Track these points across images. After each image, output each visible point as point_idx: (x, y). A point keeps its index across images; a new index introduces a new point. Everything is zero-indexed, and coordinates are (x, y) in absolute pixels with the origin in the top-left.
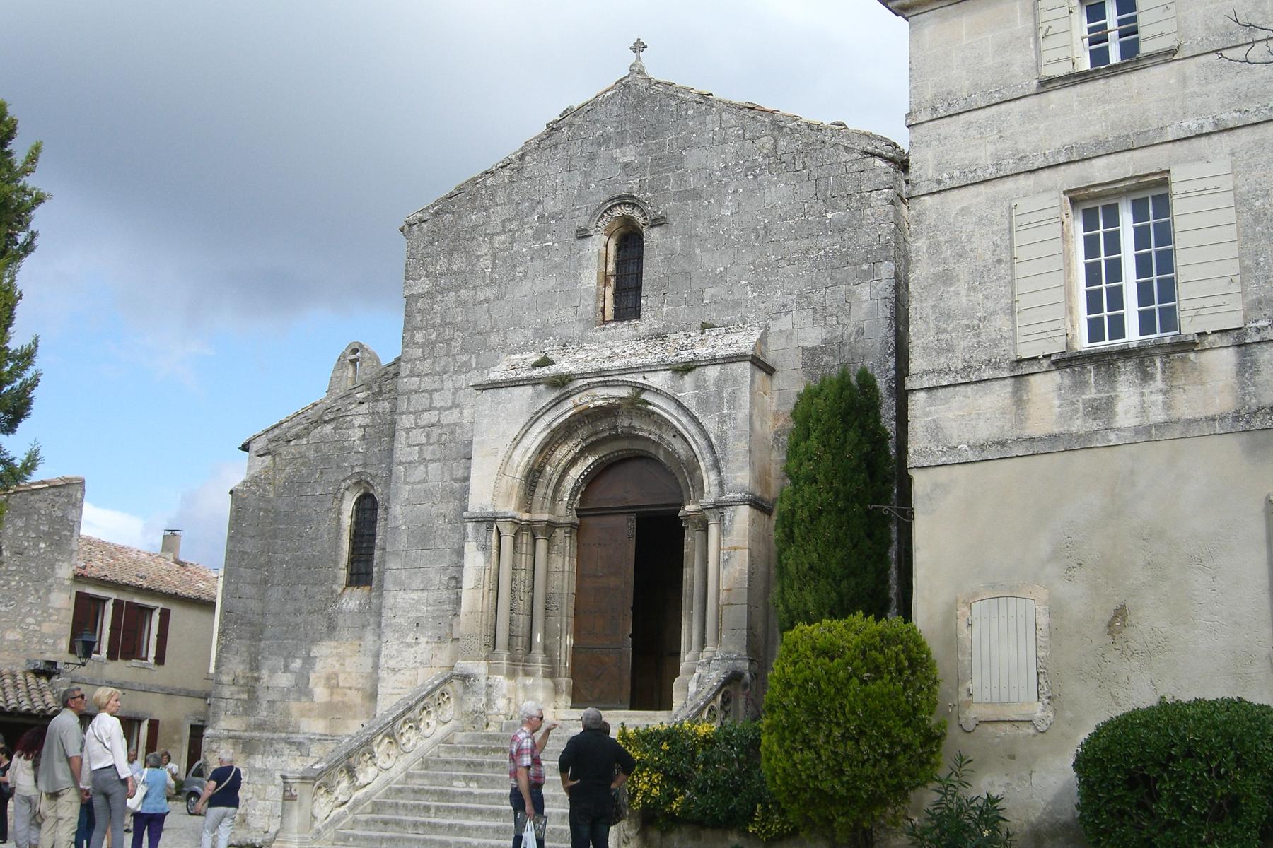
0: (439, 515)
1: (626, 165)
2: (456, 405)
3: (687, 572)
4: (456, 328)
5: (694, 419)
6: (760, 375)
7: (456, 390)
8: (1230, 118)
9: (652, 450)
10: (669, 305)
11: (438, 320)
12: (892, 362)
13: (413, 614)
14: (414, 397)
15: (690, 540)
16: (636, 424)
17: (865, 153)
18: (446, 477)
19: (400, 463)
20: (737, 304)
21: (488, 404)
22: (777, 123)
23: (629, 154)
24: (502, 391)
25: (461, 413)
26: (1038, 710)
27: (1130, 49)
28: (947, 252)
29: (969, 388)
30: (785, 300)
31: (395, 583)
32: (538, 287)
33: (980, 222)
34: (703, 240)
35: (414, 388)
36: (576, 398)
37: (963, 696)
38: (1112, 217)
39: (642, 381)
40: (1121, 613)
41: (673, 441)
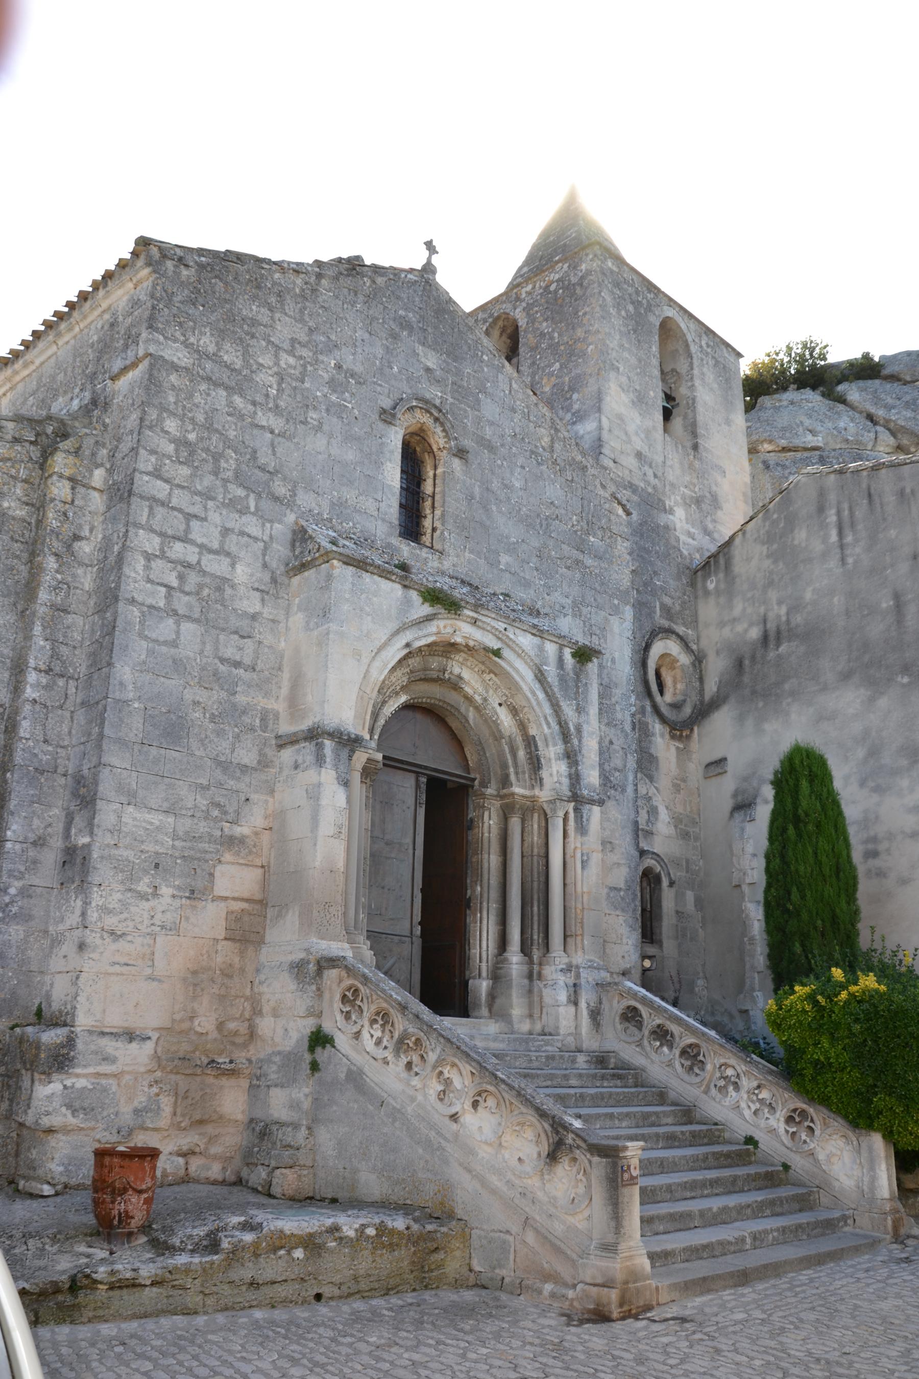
0: (196, 703)
1: (428, 370)
4: (227, 443)
5: (550, 696)
7: (226, 532)
10: (471, 552)
11: (200, 418)
13: (150, 847)
14: (160, 511)
16: (466, 674)
18: (209, 648)
19: (133, 601)
21: (348, 586)
23: (431, 360)
24: (367, 577)
25: (233, 565)
30: (565, 601)
31: (120, 788)
32: (335, 451)
35: (162, 496)
41: (498, 708)
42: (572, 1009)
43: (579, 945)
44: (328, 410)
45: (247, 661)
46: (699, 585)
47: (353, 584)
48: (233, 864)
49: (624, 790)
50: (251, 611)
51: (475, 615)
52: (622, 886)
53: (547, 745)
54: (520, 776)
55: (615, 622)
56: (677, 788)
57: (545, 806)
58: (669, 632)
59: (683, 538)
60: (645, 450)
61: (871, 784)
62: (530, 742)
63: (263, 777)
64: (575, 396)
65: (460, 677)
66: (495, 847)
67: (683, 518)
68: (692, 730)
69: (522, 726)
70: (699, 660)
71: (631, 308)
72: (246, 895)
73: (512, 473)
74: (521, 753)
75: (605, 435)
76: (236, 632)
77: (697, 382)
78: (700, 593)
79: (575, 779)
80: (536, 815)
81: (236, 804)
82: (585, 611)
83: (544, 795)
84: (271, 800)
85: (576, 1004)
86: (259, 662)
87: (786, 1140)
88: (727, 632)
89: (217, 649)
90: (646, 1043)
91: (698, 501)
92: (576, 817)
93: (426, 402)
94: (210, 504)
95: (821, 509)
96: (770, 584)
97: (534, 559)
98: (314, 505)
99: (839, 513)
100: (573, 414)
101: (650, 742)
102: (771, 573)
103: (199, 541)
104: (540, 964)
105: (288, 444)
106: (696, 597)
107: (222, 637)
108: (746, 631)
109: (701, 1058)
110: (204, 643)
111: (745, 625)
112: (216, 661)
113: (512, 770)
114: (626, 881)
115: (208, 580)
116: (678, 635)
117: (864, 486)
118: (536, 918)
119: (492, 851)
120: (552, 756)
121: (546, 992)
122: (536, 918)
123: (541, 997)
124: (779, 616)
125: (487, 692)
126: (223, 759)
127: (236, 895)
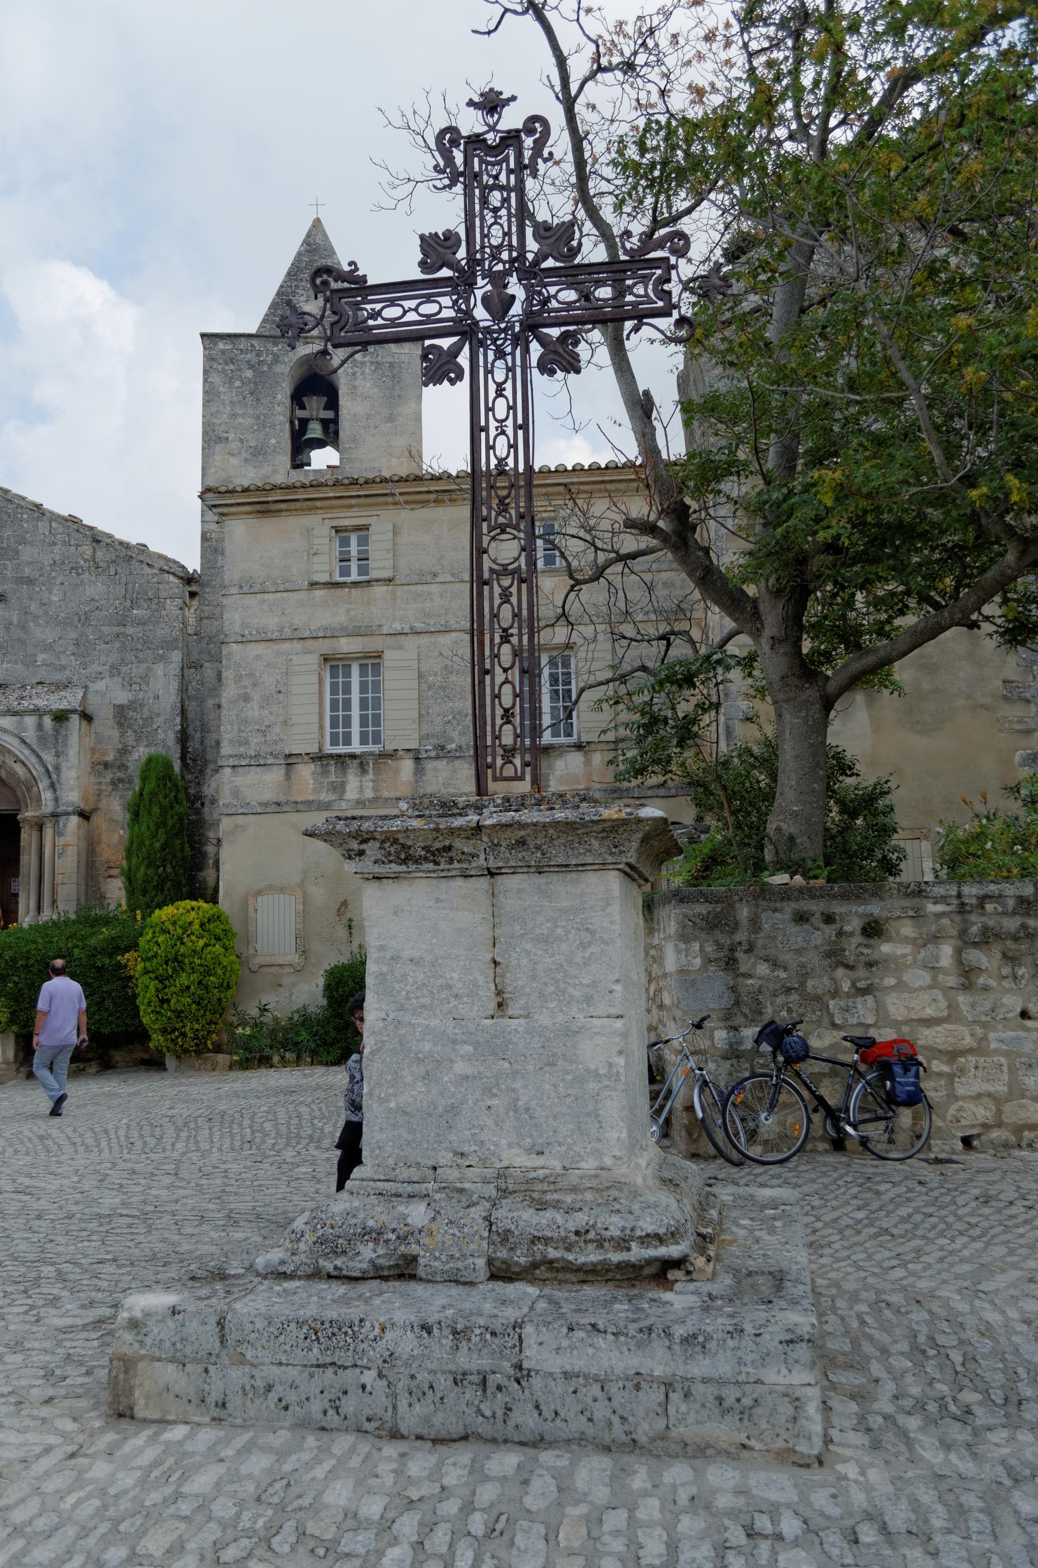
3: (24, 859)
5: (34, 751)
6: (84, 723)
8: (419, 626)
12: (178, 720)
15: (27, 837)
17: (162, 570)
20: (63, 668)
22: (97, 538)
26: (295, 959)
27: (363, 570)
28: (246, 682)
30: (100, 669)
33: (268, 665)
34: (36, 617)
37: (251, 951)
38: (348, 674)
40: (345, 904)
55: (159, 669)
71: (249, 374)
82: (123, 669)
97: (72, 648)
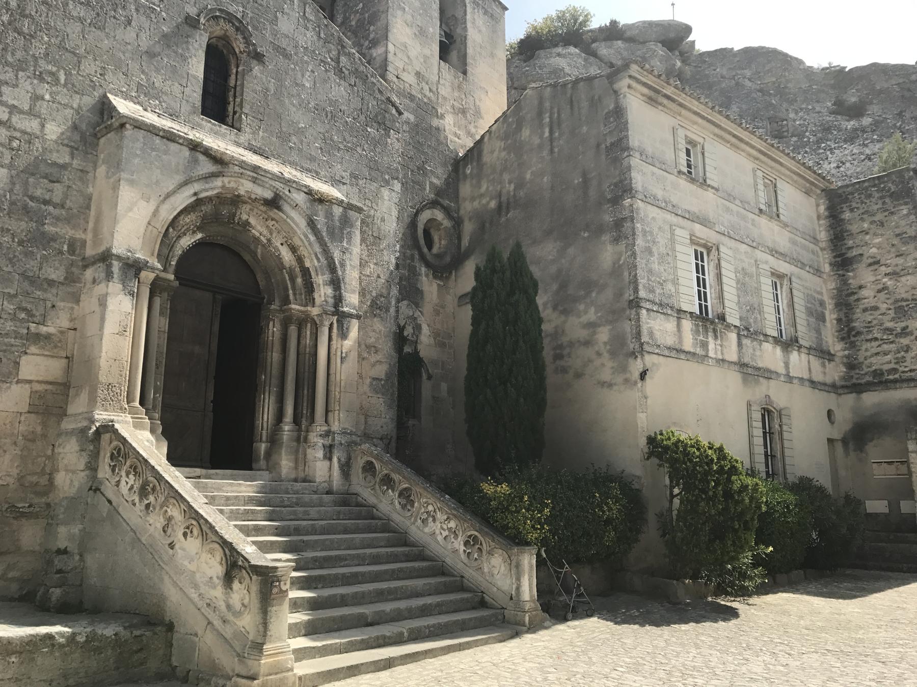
2: (31, 113)
9: (252, 247)
16: (252, 221)
21: (139, 145)
25: (43, 126)
29: (662, 316)
36: (226, 180)
39: (287, 193)
41: (280, 247)
42: (328, 463)
43: (337, 418)
44: (137, 10)
45: (57, 199)
46: (461, 171)
47: (145, 144)
48: (38, 355)
49: (387, 310)
50: (61, 161)
51: (255, 175)
52: (383, 377)
53: (317, 275)
54: (298, 297)
55: (385, 193)
56: (437, 313)
57: (315, 318)
58: (434, 204)
59: (450, 137)
60: (423, 71)
61: (561, 308)
62: (306, 272)
63: (70, 289)
64: (372, 28)
65: (247, 223)
66: (277, 347)
67: (452, 123)
68: (451, 273)
69: (300, 260)
70: (458, 223)
72: (50, 379)
73: (303, 76)
74: (299, 280)
75: (391, 57)
76: (46, 177)
77: (469, 25)
78: (461, 176)
79: (338, 300)
80: (309, 325)
81: (42, 308)
83: (315, 311)
84: (76, 307)
85: (330, 459)
86: (68, 202)
87: (463, 556)
88: (476, 204)
89: (26, 189)
90: (377, 486)
91: (463, 112)
92: (338, 326)
93: (228, 14)
94: (21, 74)
95: (540, 114)
96: (505, 169)
98: (123, 83)
99: (551, 117)
100: (370, 42)
101: (417, 280)
102: (506, 160)
103: (11, 102)
104: (307, 431)
105: (99, 32)
106: (458, 180)
107: (31, 180)
108: (488, 203)
109: (412, 498)
110: (14, 184)
111: (488, 199)
112: (26, 198)
113: (291, 292)
114: (387, 374)
115: (18, 135)
116: (443, 207)
117: (568, 95)
118: (305, 398)
119: (275, 349)
120: (321, 282)
121: (309, 451)
122: (305, 398)
123: (305, 455)
124: (509, 192)
125: (271, 234)
126: (31, 274)
127: (41, 379)
